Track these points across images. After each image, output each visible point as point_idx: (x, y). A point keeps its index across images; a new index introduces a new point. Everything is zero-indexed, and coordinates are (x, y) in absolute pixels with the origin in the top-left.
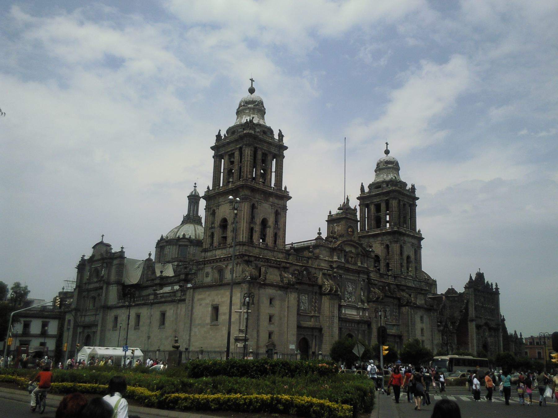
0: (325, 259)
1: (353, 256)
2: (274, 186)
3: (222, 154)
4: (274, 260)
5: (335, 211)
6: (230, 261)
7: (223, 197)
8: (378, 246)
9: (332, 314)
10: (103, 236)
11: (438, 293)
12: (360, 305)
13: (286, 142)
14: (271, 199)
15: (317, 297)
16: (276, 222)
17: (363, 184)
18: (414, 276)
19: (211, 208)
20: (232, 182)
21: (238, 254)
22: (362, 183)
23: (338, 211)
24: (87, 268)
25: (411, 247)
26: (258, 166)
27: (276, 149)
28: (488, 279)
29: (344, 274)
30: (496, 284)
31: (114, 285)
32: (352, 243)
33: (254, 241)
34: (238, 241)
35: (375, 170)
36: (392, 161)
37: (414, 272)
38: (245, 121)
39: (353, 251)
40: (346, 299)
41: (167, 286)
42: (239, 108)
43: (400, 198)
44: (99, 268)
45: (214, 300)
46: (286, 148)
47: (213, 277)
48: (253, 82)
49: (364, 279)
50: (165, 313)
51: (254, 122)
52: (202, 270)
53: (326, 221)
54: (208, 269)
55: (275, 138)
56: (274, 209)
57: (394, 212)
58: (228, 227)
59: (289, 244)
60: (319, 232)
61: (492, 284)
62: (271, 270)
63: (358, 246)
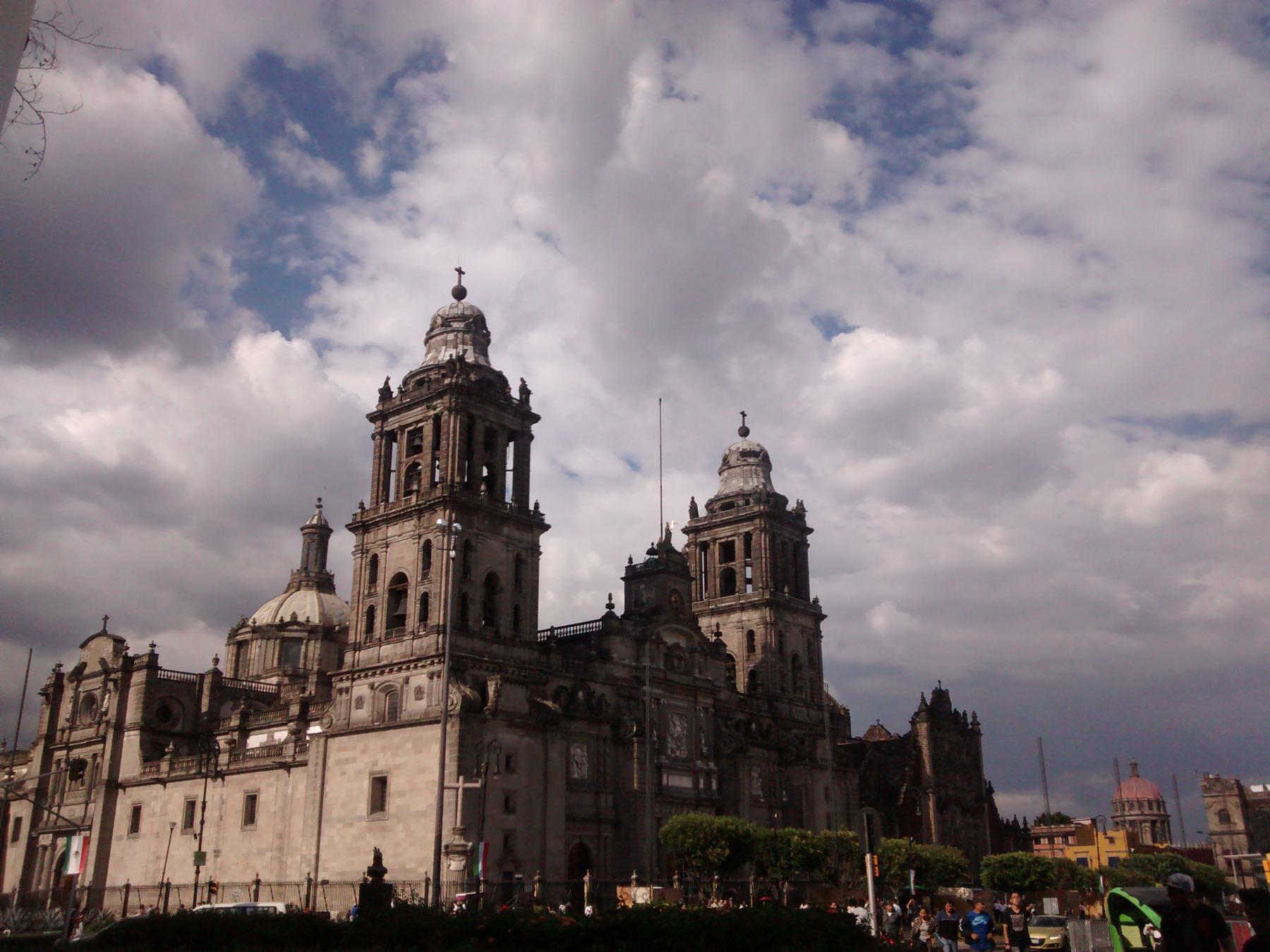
0: (623, 662)
1: (682, 654)
2: (511, 502)
3: (393, 430)
5: (640, 558)
6: (415, 672)
7: (397, 527)
8: (731, 634)
10: (106, 618)
11: (853, 737)
12: (699, 763)
13: (535, 406)
14: (506, 530)
15: (608, 750)
16: (518, 580)
17: (695, 500)
18: (809, 699)
19: (368, 551)
20: (418, 491)
21: (433, 653)
22: (693, 498)
23: (648, 557)
24: (69, 693)
25: (801, 635)
26: (476, 458)
27: (515, 419)
28: (958, 703)
30: (974, 714)
31: (132, 733)
33: (471, 623)
34: (432, 624)
35: (720, 469)
37: (808, 690)
38: (447, 358)
39: (683, 644)
40: (670, 752)
41: (258, 732)
42: (432, 330)
43: (776, 531)
44: (98, 693)
45: (375, 763)
46: (536, 418)
47: (373, 712)
48: (462, 275)
49: (706, 706)
50: (256, 796)
51: (467, 360)
52: (347, 693)
53: (622, 578)
54: (361, 688)
55: (513, 396)
56: (513, 551)
57: (764, 560)
58: (409, 592)
59: (544, 631)
60: (608, 602)
61: (965, 714)
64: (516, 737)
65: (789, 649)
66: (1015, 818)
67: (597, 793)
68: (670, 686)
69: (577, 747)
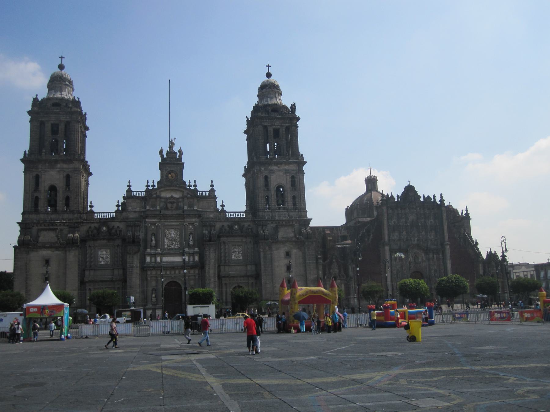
0: (135, 210)
1: (175, 201)
4: (59, 222)
9: (129, 265)
12: (187, 250)
14: (59, 166)
16: (68, 184)
18: (290, 206)
22: (247, 117)
25: (285, 176)
27: (68, 116)
29: (159, 222)
30: (441, 195)
32: (172, 188)
33: (39, 208)
36: (267, 84)
39: (177, 195)
43: (266, 124)
48: (63, 59)
49: (193, 222)
60: (128, 184)
61: (434, 197)
62: (43, 233)
63: (182, 189)
64: (50, 252)
65: (273, 184)
66: (490, 250)
67: (113, 269)
68: (165, 217)
69: (103, 251)
